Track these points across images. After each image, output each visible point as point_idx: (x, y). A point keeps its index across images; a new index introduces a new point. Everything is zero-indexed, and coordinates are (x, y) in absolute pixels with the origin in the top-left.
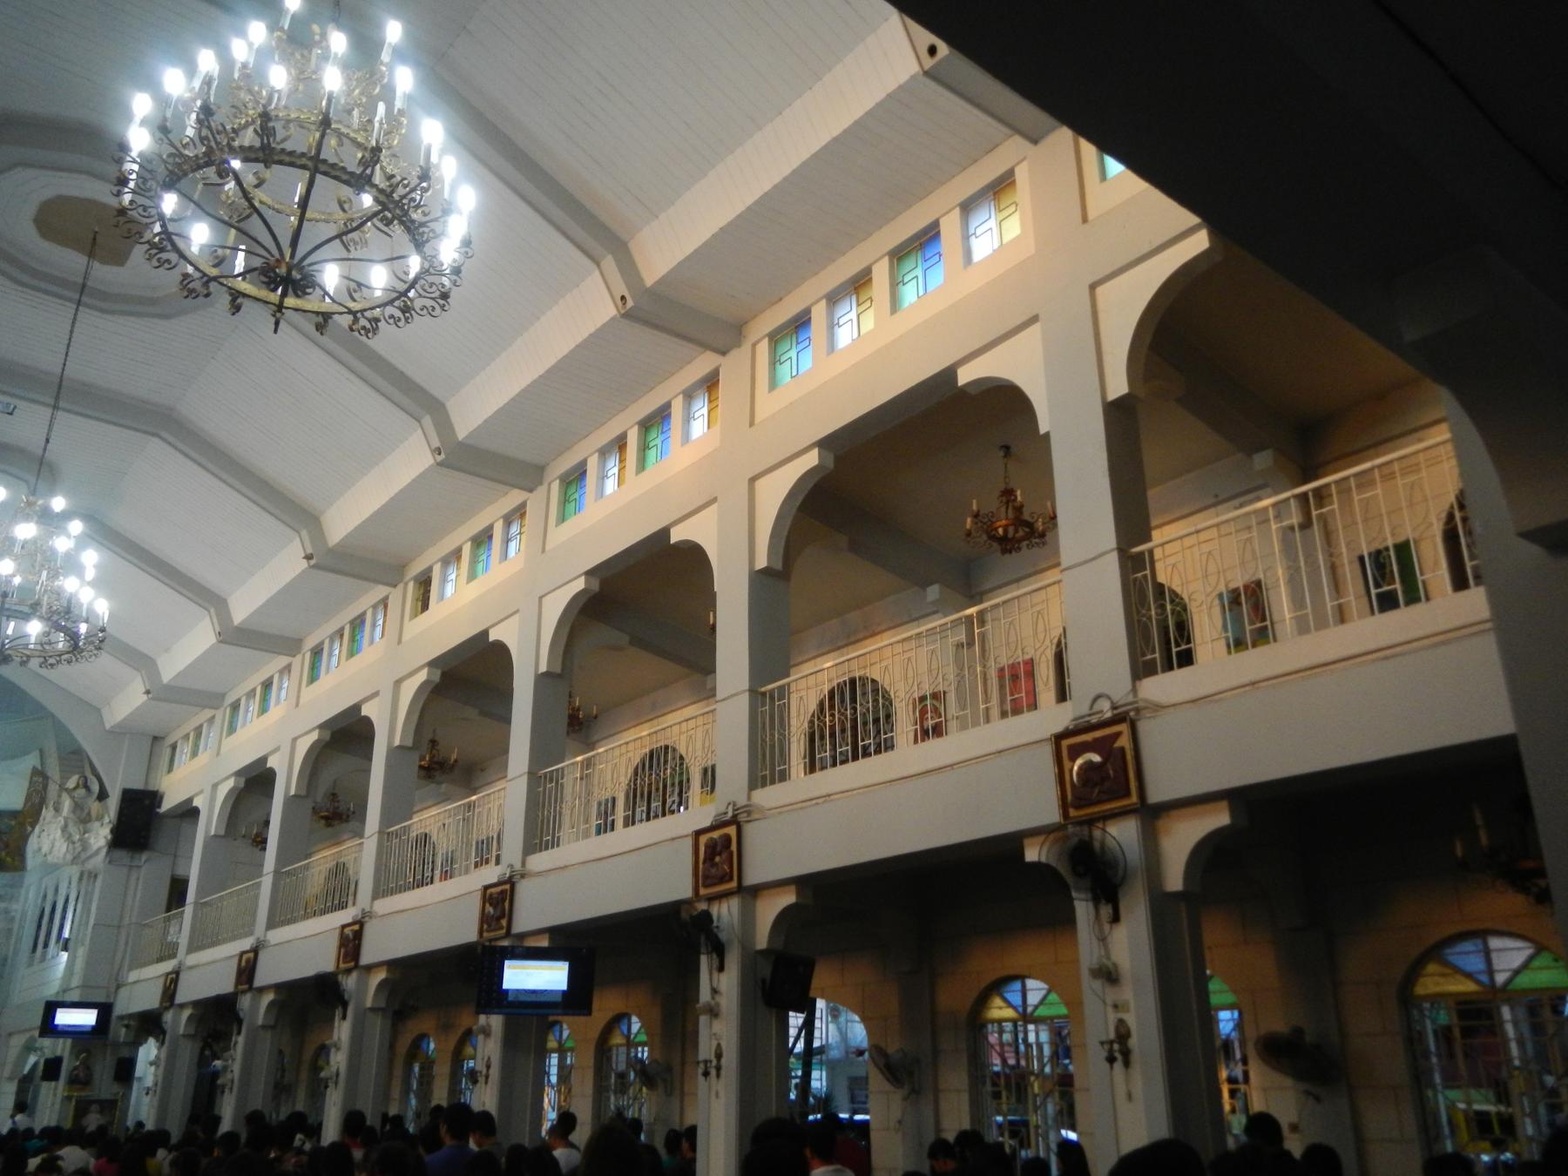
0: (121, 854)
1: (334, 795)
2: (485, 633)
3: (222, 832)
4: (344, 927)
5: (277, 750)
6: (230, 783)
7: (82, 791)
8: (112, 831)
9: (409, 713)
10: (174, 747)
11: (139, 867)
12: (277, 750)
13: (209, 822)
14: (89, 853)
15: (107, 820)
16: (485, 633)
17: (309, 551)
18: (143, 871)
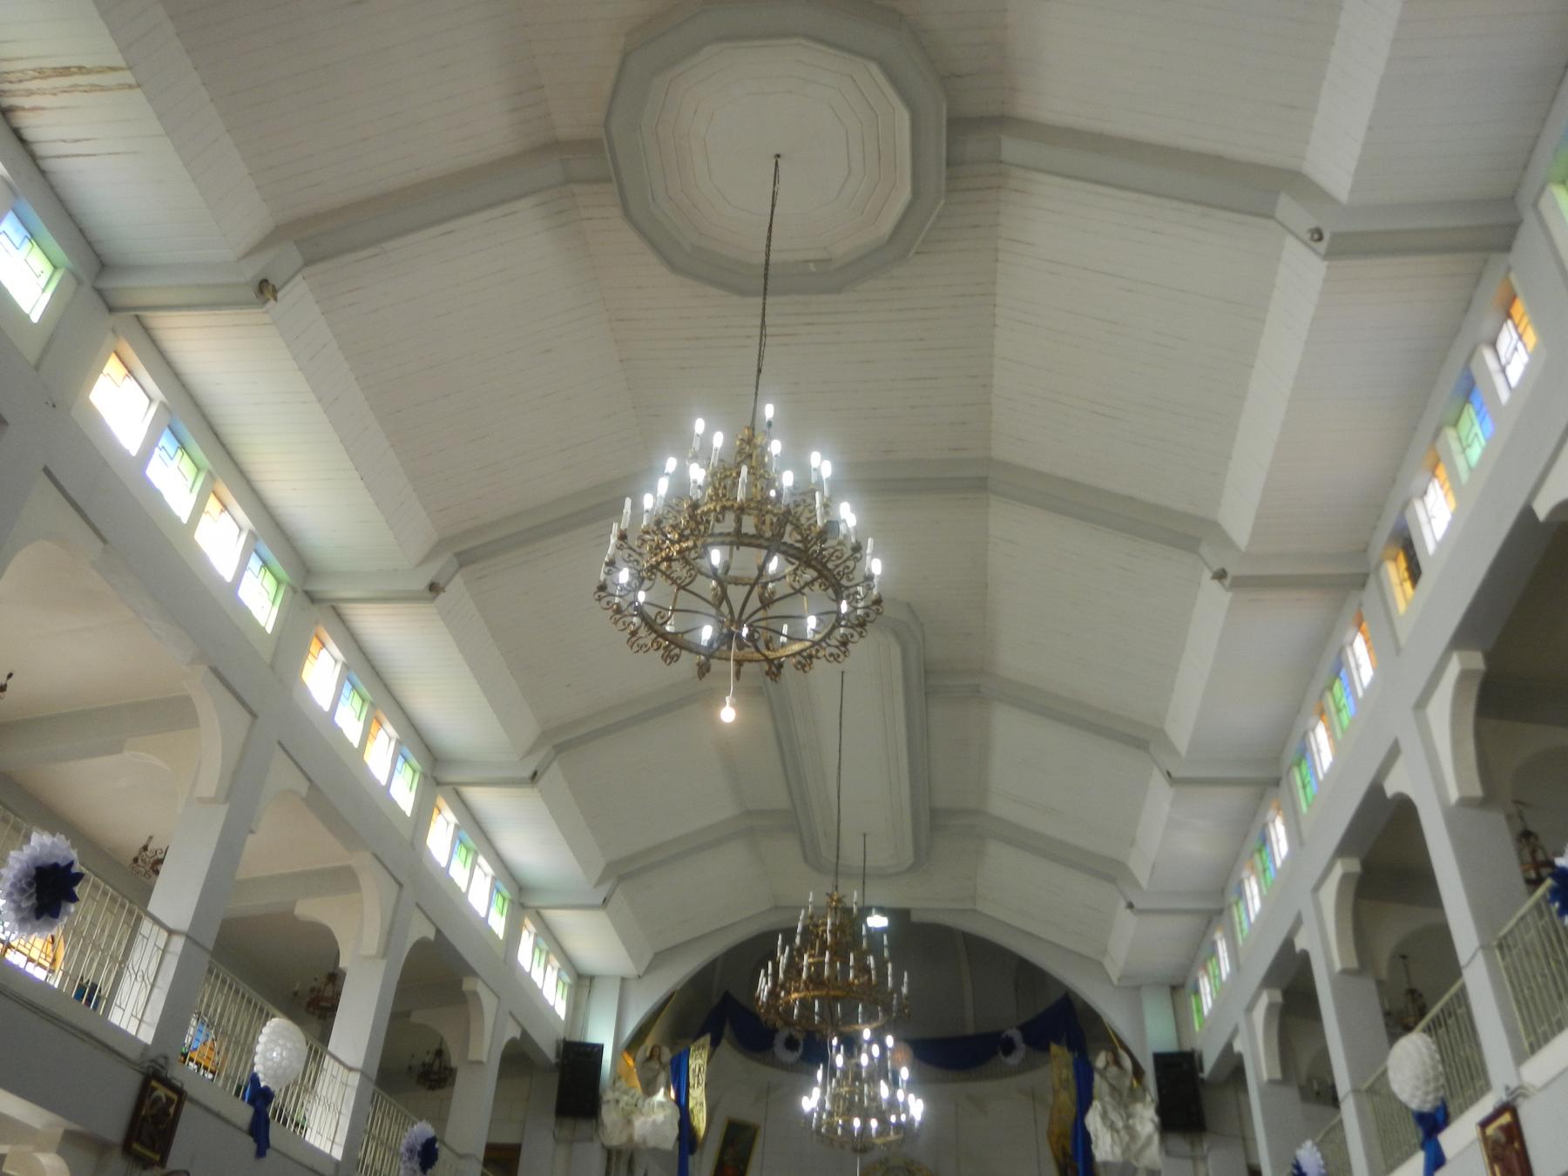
0: (1179, 1143)
1: (1412, 992)
2: (1527, 513)
3: (1278, 1075)
4: (1484, 1125)
5: (1298, 922)
6: (1264, 1001)
7: (1113, 1070)
8: (1161, 1111)
9: (1456, 743)
10: (1197, 992)
11: (1204, 1159)
12: (1298, 922)
13: (1260, 1066)
14: (1139, 1144)
15: (1148, 1098)
16: (1527, 513)
17: (1216, 568)
18: (1210, 1162)
